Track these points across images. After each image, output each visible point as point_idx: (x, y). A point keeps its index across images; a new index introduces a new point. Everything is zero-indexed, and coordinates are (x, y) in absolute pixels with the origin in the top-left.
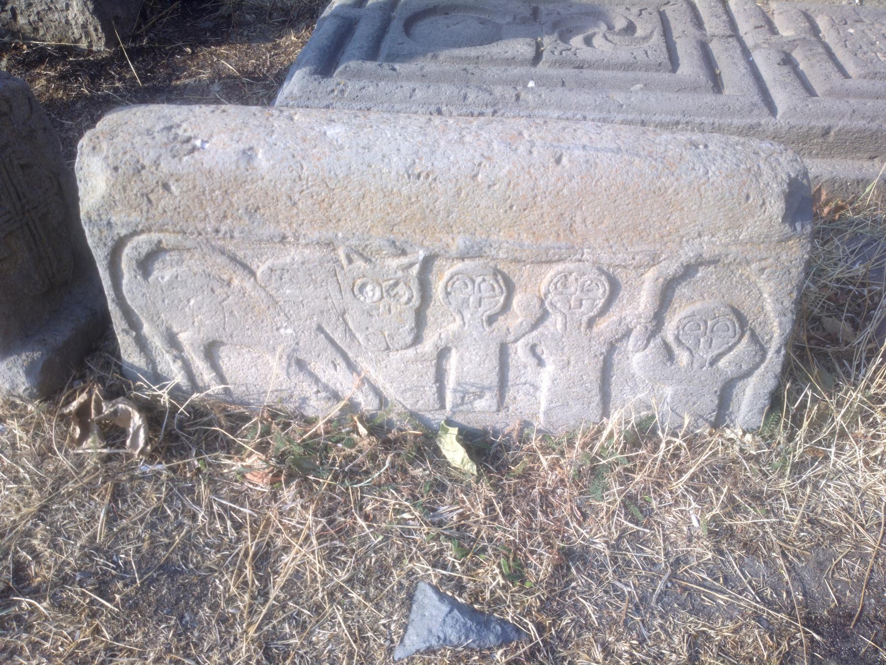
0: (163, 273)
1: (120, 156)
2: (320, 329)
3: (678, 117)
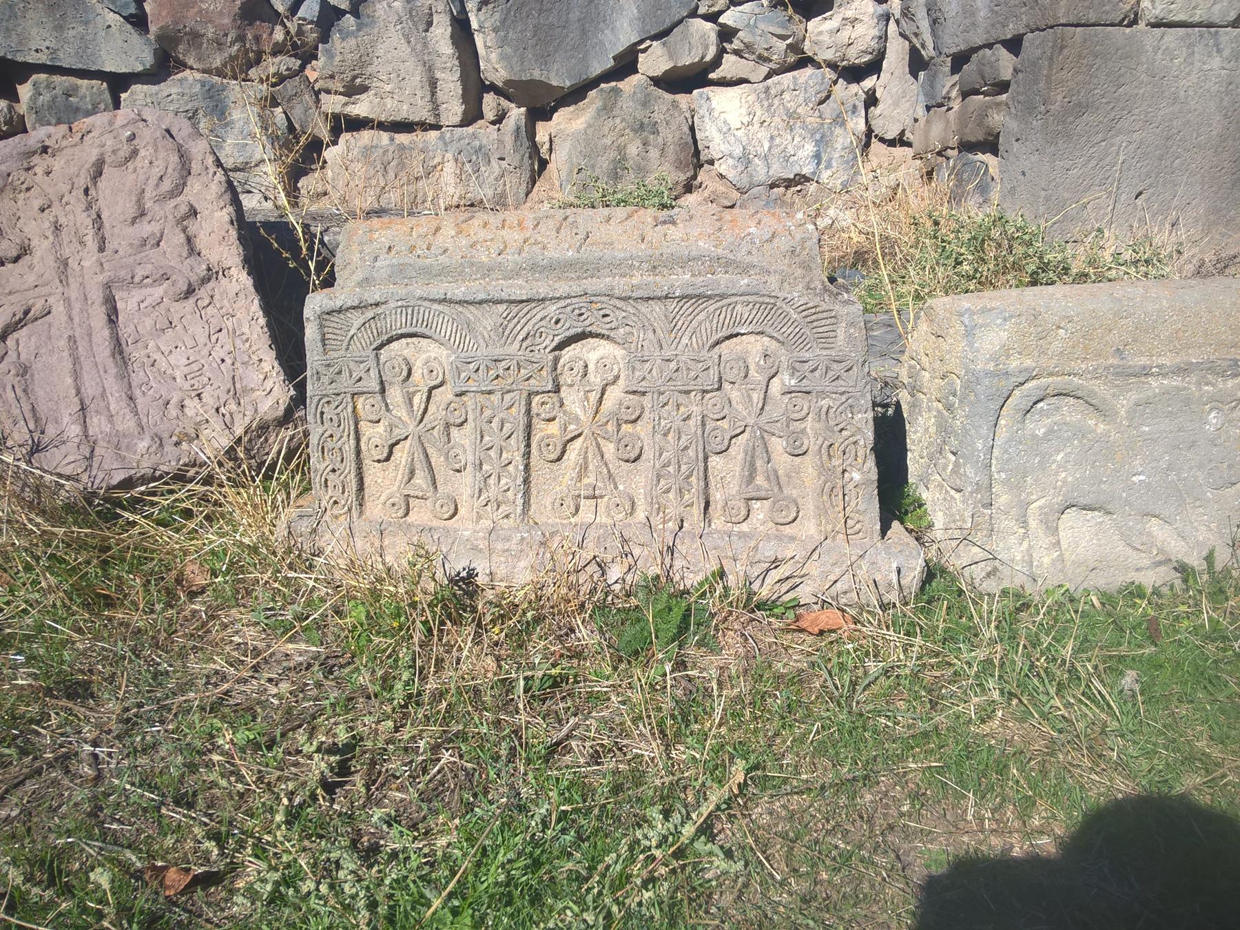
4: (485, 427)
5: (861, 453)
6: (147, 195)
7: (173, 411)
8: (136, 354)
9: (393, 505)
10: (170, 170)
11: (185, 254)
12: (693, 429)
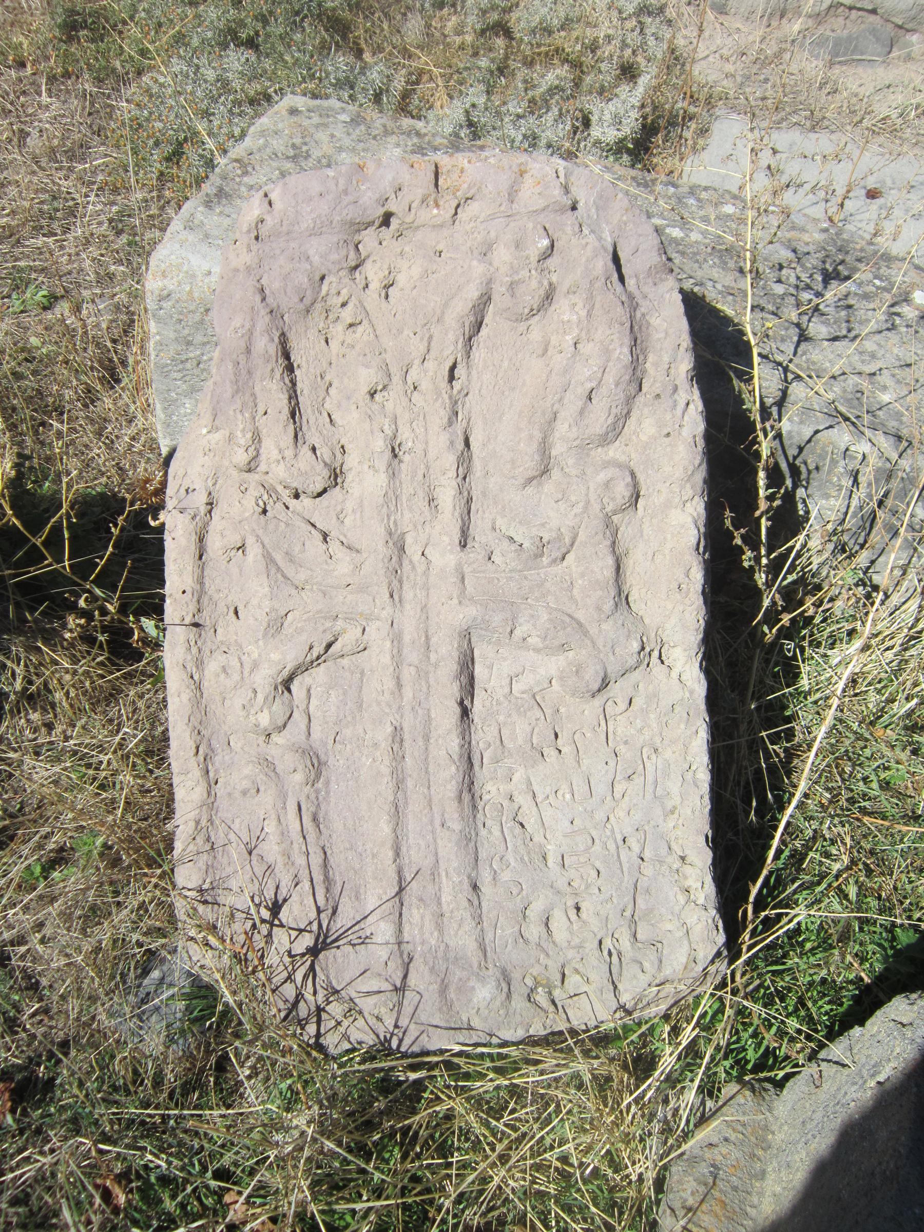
6: (562, 428)
7: (534, 931)
8: (491, 790)
10: (610, 379)
11: (609, 605)
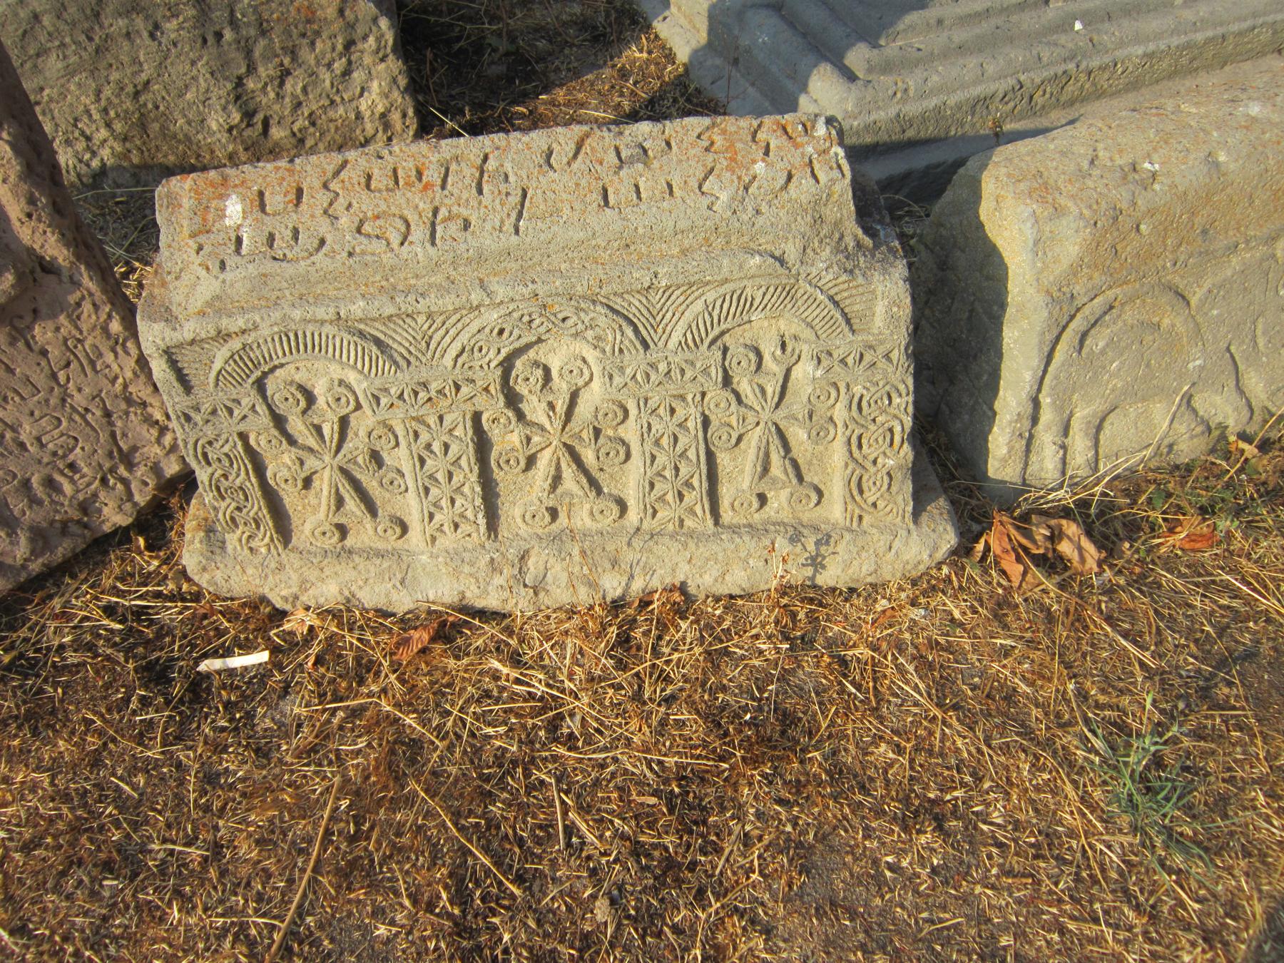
0: (1097, 342)
1: (1095, 207)
2: (1228, 350)
3: (1248, 23)
4: (425, 454)
5: (897, 439)
9: (324, 533)
12: (693, 432)
